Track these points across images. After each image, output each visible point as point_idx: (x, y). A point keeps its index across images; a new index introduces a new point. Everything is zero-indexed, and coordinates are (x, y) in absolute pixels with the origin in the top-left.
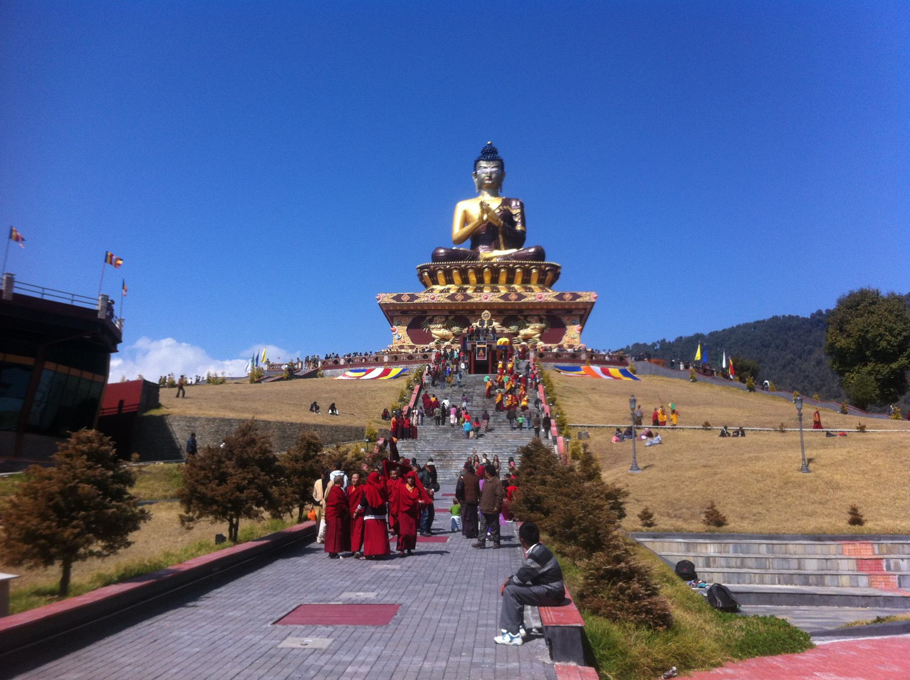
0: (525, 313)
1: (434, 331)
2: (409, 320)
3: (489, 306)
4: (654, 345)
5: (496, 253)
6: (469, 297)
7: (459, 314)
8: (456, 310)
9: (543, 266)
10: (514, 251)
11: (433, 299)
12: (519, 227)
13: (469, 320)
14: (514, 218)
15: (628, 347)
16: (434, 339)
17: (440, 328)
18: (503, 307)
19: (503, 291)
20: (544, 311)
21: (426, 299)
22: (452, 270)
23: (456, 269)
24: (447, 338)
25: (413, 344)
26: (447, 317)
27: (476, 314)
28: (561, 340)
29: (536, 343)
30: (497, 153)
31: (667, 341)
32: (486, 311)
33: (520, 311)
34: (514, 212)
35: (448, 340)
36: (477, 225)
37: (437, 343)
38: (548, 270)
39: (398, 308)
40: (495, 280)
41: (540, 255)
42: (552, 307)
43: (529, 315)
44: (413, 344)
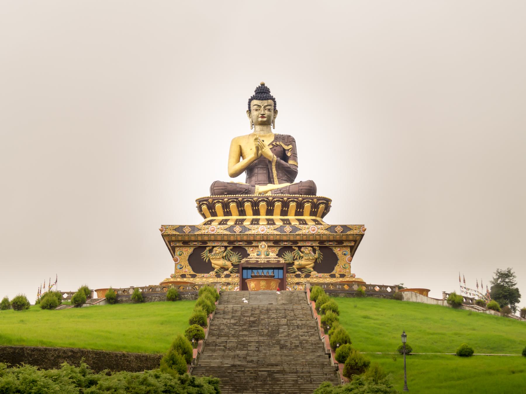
0: (300, 244)
1: (212, 261)
2: (190, 250)
3: (265, 239)
5: (270, 187)
6: (245, 229)
7: (237, 244)
8: (234, 241)
9: (315, 200)
10: (288, 184)
11: (213, 231)
12: (291, 162)
13: (246, 251)
14: (286, 152)
16: (213, 269)
17: (219, 258)
18: (278, 238)
19: (279, 224)
20: (318, 242)
21: (206, 231)
22: (229, 202)
23: (233, 201)
24: (226, 267)
25: (194, 273)
26: (226, 247)
27: (253, 245)
28: (333, 269)
29: (310, 273)
30: (270, 92)
32: (264, 243)
33: (295, 242)
34: (286, 148)
35: (227, 269)
36: (252, 160)
37: (216, 273)
38: (320, 204)
39: (180, 238)
40: (270, 212)
41: (311, 189)
42: (325, 238)
43: (304, 246)
44: (194, 273)
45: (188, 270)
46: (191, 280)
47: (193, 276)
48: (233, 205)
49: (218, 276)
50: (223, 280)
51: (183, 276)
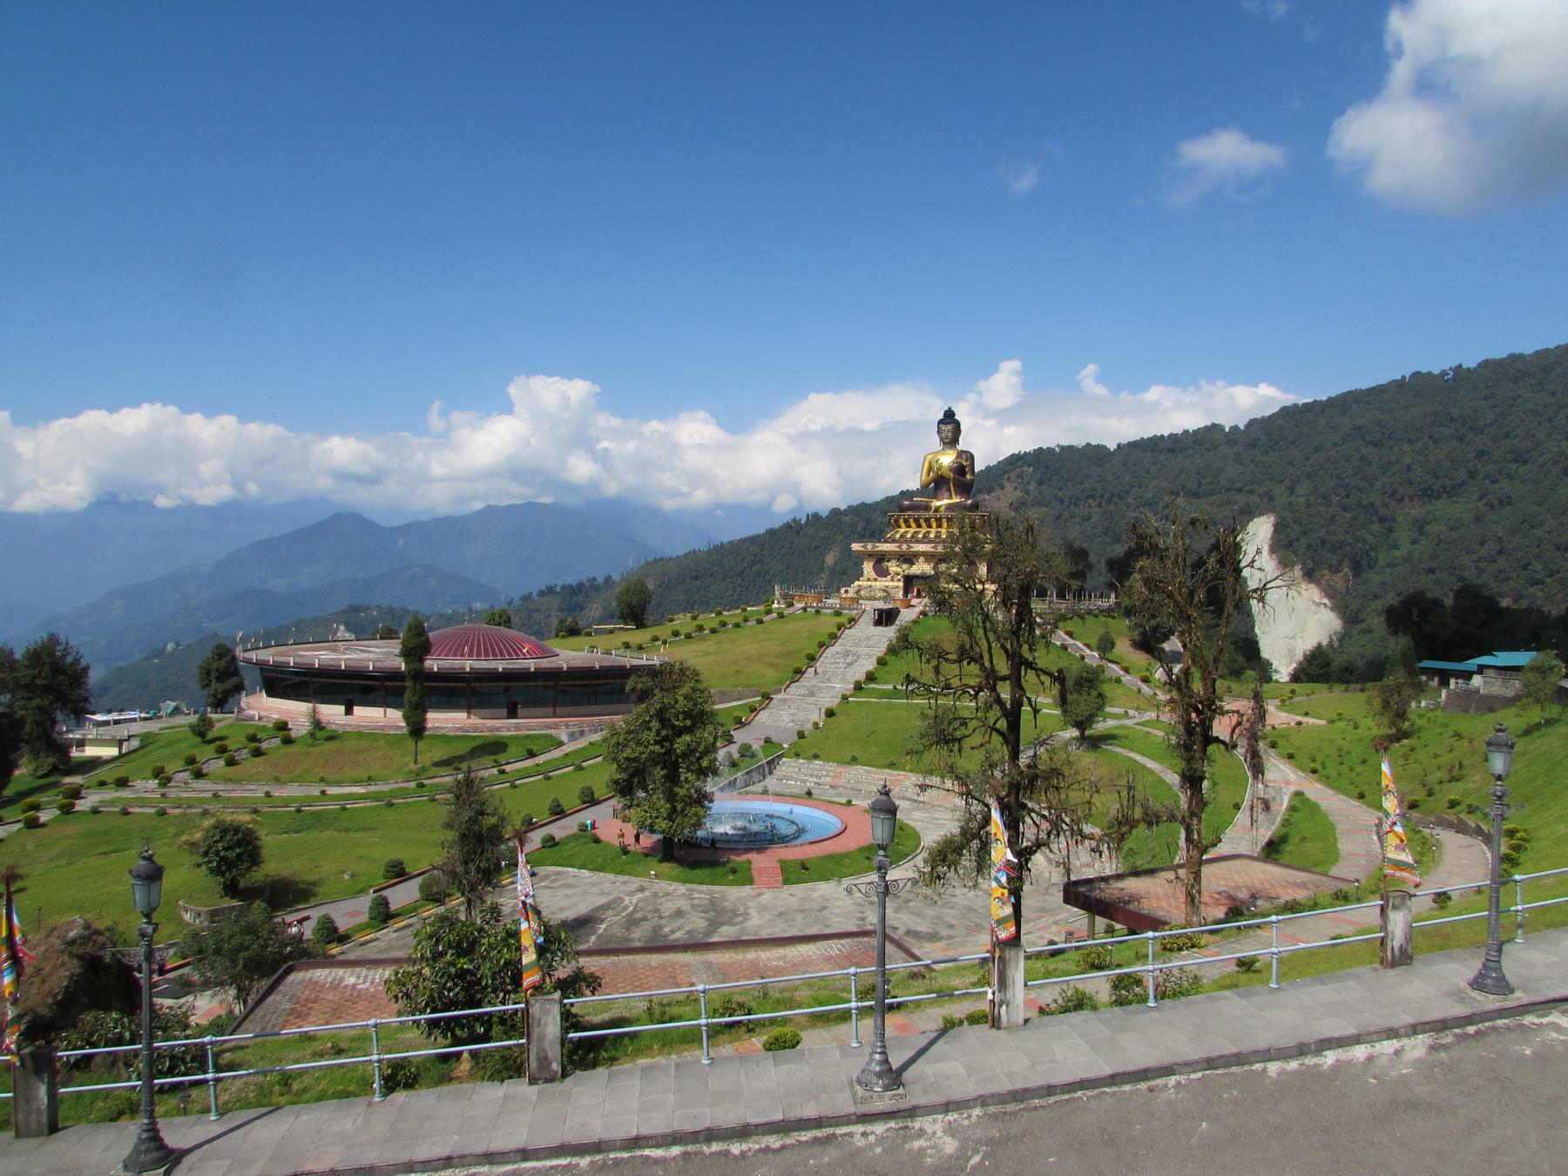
4: (1444, 373)
5: (946, 501)
15: (1404, 377)
31: (1464, 367)
40: (939, 526)
45: (873, 575)
46: (873, 583)
47: (876, 580)
49: (893, 580)
50: (896, 584)
51: (869, 580)
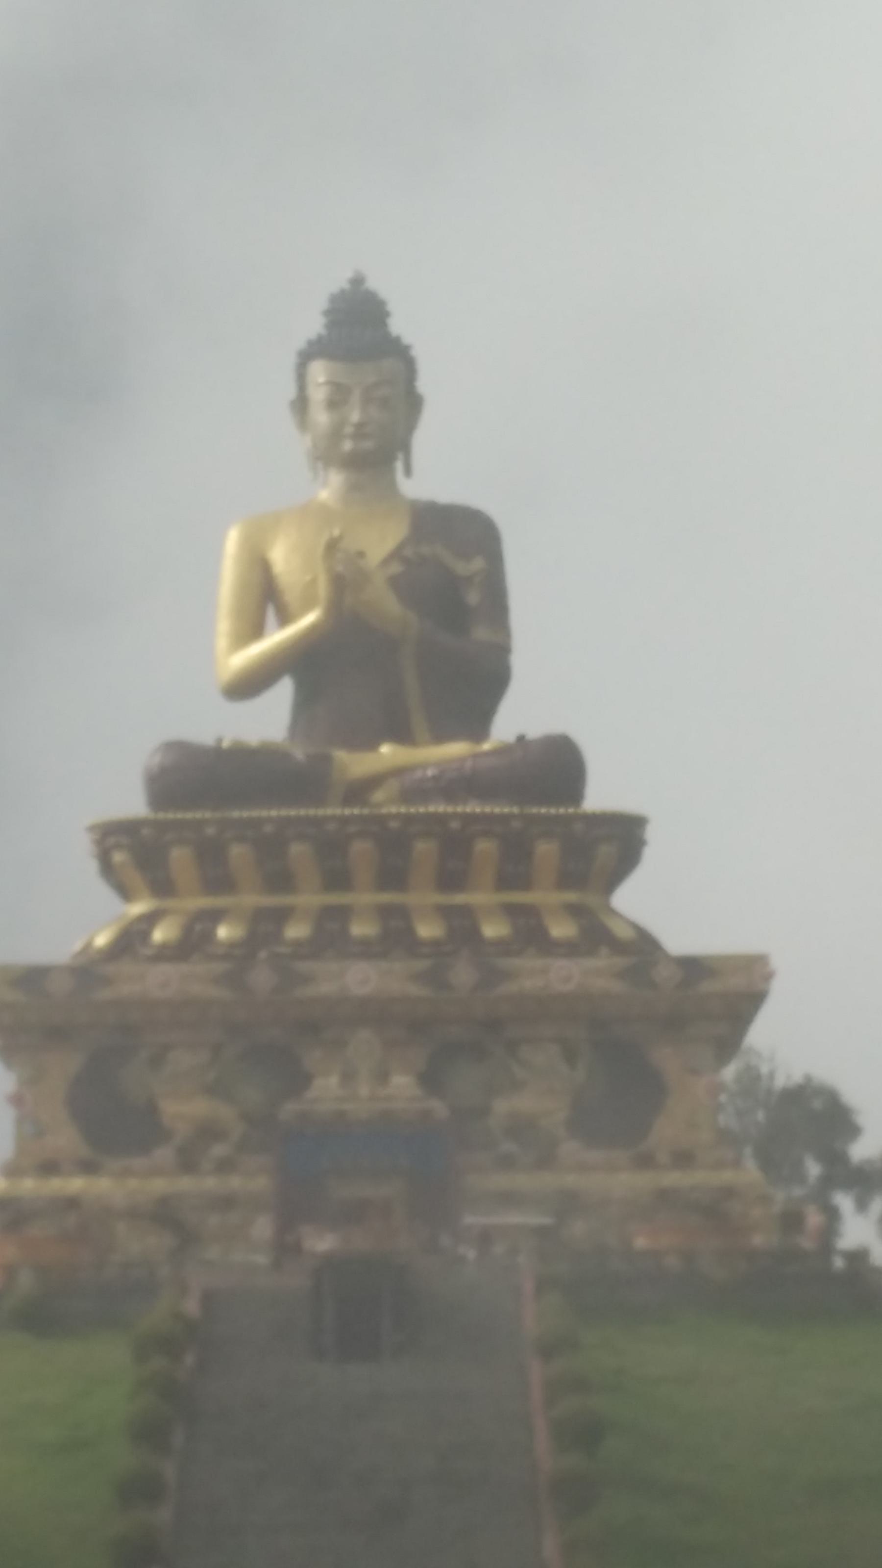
12: (481, 633)
34: (461, 568)
47: (88, 1168)
48: (238, 852)
50: (210, 1183)
